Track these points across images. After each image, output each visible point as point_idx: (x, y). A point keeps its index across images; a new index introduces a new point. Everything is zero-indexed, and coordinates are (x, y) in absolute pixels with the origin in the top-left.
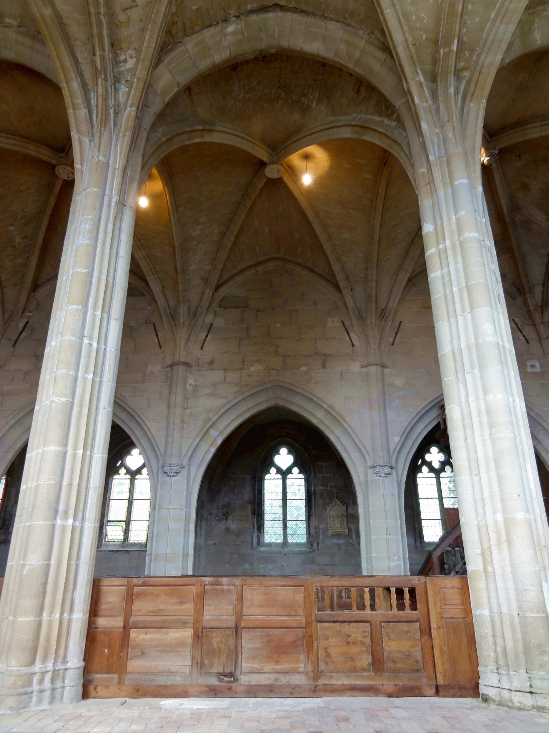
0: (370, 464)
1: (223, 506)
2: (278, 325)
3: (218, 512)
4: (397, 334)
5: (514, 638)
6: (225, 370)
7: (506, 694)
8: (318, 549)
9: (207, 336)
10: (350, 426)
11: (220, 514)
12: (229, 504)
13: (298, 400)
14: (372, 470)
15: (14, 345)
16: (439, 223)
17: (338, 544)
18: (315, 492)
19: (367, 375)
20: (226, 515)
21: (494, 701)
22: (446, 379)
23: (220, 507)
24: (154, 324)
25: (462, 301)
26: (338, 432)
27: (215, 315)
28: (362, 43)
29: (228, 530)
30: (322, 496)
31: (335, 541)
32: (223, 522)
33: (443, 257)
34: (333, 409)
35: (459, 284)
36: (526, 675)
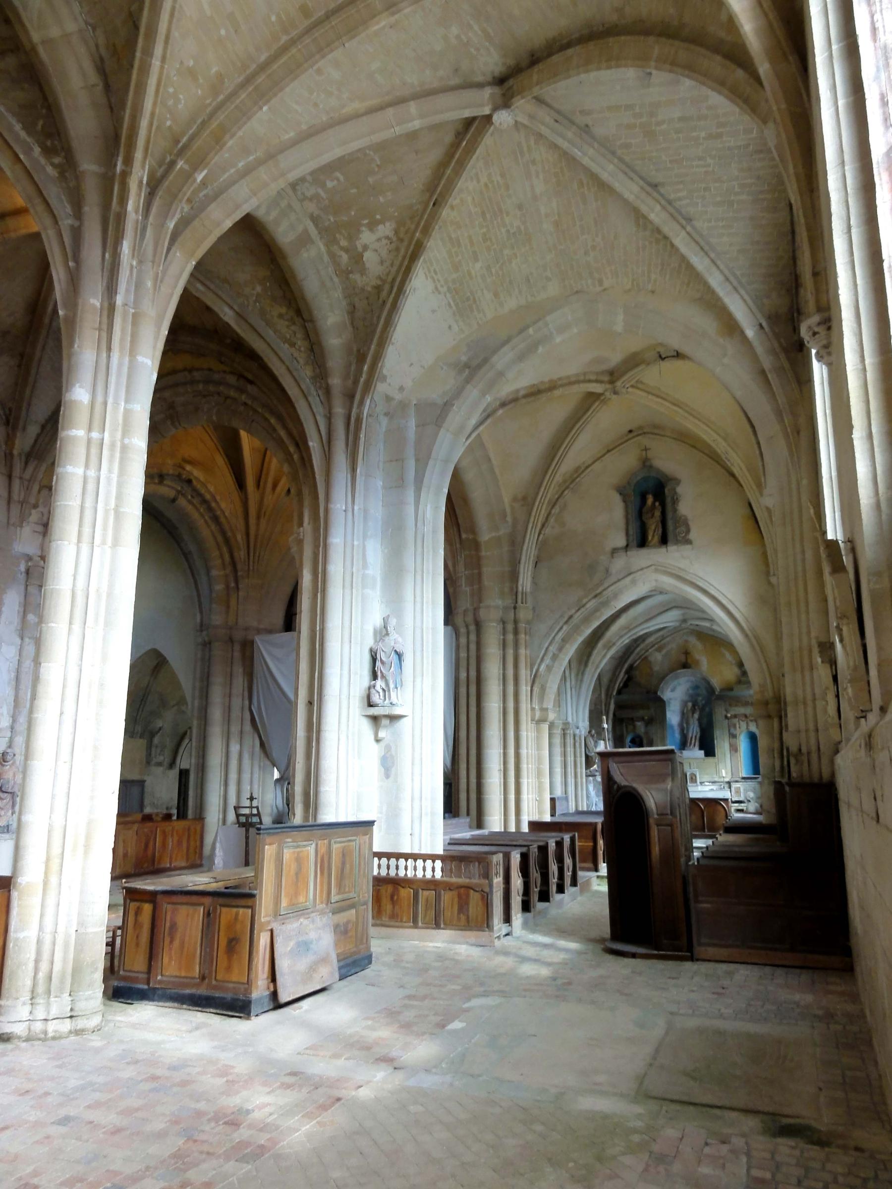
5: (65, 960)
7: (38, 1027)
16: (100, 399)
21: (19, 1038)
22: (53, 625)
25: (105, 528)
28: (71, 27)
33: (94, 451)
35: (107, 504)
36: (70, 999)
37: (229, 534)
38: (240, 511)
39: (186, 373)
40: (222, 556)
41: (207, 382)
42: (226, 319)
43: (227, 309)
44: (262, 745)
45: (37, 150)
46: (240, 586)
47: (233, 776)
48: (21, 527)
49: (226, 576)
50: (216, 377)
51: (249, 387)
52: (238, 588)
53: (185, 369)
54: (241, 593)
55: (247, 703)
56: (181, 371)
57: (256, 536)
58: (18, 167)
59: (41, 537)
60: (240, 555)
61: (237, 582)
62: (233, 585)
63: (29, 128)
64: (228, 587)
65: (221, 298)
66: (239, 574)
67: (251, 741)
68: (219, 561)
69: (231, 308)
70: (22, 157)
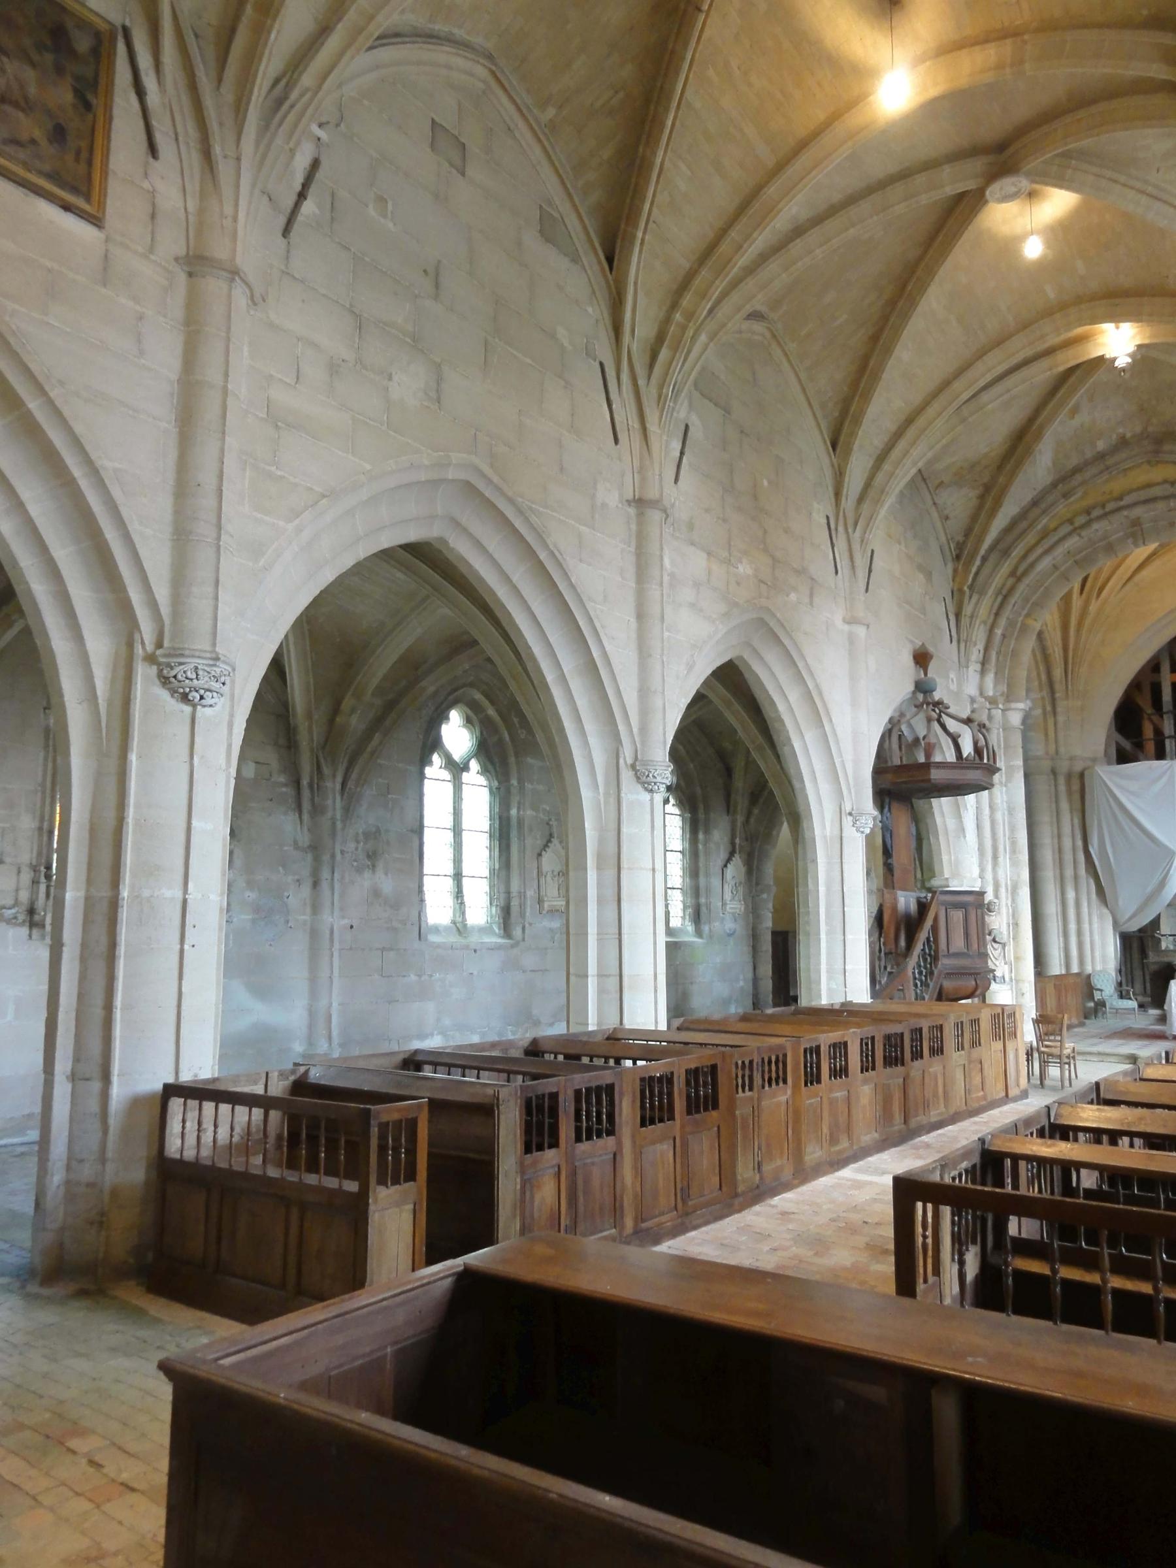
0: (848, 809)
1: (367, 835)
2: (766, 483)
3: (357, 849)
4: (870, 571)
6: (709, 554)
8: (524, 940)
9: (682, 453)
12: (378, 830)
13: (772, 657)
14: (850, 818)
15: (286, 231)
17: (551, 930)
23: (361, 837)
24: (601, 364)
26: (810, 736)
29: (376, 893)
30: (531, 830)
32: (367, 874)
34: (820, 694)
37: (1050, 651)
38: (1058, 624)
39: (1167, 486)
40: (1039, 675)
46: (1059, 709)
47: (1072, 927)
48: (967, 667)
49: (1043, 698)
52: (1055, 713)
53: (1165, 481)
54: (1061, 719)
55: (1080, 843)
56: (1158, 484)
59: (978, 676)
60: (1058, 673)
62: (1049, 708)
64: (1045, 713)
66: (1057, 695)
68: (1036, 683)
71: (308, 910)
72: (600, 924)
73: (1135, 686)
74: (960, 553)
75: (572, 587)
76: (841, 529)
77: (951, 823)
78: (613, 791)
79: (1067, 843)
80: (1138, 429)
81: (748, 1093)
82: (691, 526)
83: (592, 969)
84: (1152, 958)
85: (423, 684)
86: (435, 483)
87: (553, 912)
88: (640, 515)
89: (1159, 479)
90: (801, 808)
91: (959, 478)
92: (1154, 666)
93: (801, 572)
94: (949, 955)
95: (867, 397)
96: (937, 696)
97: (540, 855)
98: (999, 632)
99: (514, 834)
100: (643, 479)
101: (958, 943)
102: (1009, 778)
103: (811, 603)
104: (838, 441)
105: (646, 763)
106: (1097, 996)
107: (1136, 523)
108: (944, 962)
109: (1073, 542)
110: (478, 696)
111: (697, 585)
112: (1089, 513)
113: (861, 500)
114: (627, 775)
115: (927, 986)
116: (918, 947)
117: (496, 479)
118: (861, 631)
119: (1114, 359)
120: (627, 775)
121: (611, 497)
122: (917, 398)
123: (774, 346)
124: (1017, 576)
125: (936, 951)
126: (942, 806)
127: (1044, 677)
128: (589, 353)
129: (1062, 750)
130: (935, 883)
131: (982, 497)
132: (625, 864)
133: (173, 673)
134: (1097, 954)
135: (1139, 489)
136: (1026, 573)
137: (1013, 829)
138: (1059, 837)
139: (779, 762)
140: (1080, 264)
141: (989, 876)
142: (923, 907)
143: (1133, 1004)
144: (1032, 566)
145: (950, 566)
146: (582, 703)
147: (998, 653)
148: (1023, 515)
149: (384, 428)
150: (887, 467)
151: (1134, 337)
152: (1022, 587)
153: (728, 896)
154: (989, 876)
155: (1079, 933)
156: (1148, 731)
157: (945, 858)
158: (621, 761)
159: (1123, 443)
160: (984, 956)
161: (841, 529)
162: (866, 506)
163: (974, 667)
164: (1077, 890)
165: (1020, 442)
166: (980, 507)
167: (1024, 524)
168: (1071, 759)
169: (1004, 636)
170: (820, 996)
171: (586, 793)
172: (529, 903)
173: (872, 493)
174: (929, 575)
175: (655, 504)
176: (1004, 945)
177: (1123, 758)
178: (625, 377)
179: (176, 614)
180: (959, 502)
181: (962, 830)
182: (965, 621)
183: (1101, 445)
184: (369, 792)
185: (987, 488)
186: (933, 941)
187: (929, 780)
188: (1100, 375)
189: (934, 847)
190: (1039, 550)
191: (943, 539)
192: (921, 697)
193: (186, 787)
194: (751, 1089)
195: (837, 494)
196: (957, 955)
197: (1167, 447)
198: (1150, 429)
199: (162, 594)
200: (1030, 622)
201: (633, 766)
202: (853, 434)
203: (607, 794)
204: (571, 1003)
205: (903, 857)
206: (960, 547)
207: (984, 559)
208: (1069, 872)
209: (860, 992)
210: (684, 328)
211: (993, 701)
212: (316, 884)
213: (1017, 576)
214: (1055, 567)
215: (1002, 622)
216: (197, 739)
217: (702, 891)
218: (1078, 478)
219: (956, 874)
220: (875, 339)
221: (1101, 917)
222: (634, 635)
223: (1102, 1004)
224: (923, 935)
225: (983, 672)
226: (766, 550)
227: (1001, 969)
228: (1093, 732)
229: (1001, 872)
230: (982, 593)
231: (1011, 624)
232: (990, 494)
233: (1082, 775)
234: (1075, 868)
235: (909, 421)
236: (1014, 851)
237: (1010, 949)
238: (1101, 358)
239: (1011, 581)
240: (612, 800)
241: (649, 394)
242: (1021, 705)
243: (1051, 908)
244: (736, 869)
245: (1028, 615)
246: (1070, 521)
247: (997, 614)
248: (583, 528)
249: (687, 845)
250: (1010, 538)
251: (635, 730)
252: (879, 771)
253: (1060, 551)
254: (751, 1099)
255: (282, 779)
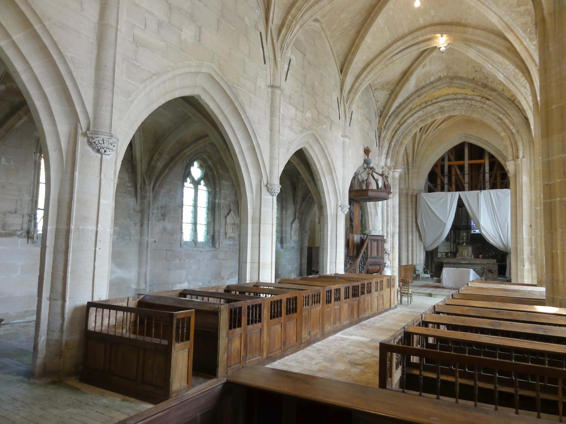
1: (162, 207)
6: (296, 109)
10: (337, 177)
11: (159, 215)
12: (166, 206)
17: (229, 245)
18: (219, 205)
19: (344, 143)
20: (164, 215)
23: (160, 208)
26: (328, 178)
27: (292, 53)
29: (165, 229)
30: (223, 208)
31: (228, 242)
32: (162, 222)
34: (332, 163)
41: (465, 99)
42: (500, 79)
43: (500, 75)
44: (420, 236)
45: (528, 40)
47: (410, 248)
50: (469, 97)
51: (488, 102)
52: (408, 173)
53: (453, 93)
54: (410, 176)
55: (414, 220)
57: (417, 152)
58: (522, 46)
59: (385, 159)
61: (408, 171)
63: (524, 31)
65: (499, 71)
66: (410, 167)
67: (416, 234)
69: (502, 74)
70: (524, 43)
71: (139, 235)
72: (252, 244)
73: (436, 165)
74: (382, 115)
75: (247, 117)
76: (342, 102)
77: (373, 211)
78: (259, 195)
79: (410, 219)
80: (446, 74)
81: (307, 307)
82: (290, 98)
83: (249, 260)
84: (436, 260)
85: (185, 151)
86: (198, 73)
87: (230, 238)
88: (273, 92)
89: (451, 92)
90: (323, 204)
91: (382, 88)
92: (442, 159)
93: (328, 117)
94: (371, 257)
95: (354, 54)
96: (371, 165)
97: (226, 217)
98: (393, 144)
99: (217, 209)
100: (274, 78)
101: (375, 254)
102: (393, 196)
103: (331, 129)
104: (343, 70)
105: (271, 185)
106: (417, 272)
107: (442, 107)
108: (369, 260)
109: (420, 113)
110: (205, 157)
111: (291, 119)
112: (426, 103)
113: (350, 92)
114: (264, 189)
115: (363, 268)
116: (361, 255)
117: (220, 73)
118: (347, 140)
119: (440, 48)
120: (264, 189)
121: (262, 84)
122: (372, 56)
123: (322, 32)
124: (400, 124)
125: (367, 256)
126: (370, 205)
127: (406, 160)
128: (256, 28)
129: (410, 187)
130: (366, 232)
131: (390, 95)
132: (262, 222)
133: (94, 141)
134: (418, 258)
135: (444, 95)
136: (403, 123)
137: (394, 214)
138: (407, 217)
139: (316, 187)
140: (432, 11)
141: (385, 230)
142: (363, 241)
143: (429, 276)
144: (406, 121)
145: (378, 119)
146: (249, 161)
147: (392, 151)
148: (404, 102)
149: (179, 50)
150: (359, 81)
151: (447, 40)
152: (402, 128)
153: (293, 234)
154: (385, 230)
155: (412, 251)
156: (439, 182)
157: (370, 223)
158: (262, 184)
159: (440, 79)
160: (383, 258)
161: (342, 102)
162: (351, 94)
163: (384, 156)
164: (412, 236)
165: (405, 75)
166: (389, 99)
167: (404, 105)
168: (413, 190)
169: (395, 145)
170: (327, 271)
171: (249, 195)
172: (221, 234)
173: (353, 90)
174: (370, 122)
175: (279, 88)
176: (389, 254)
177: (430, 190)
178: (269, 38)
179: (95, 118)
180: (382, 96)
181: (377, 214)
182: (382, 139)
183: (432, 79)
184: (163, 191)
185: (392, 92)
186: (366, 253)
187: (367, 195)
188: (434, 53)
189: (367, 219)
190: (409, 115)
191: (376, 109)
192: (366, 166)
193: (98, 186)
194: (308, 305)
195: (341, 90)
196: (374, 258)
197: (455, 81)
198: (449, 74)
199: (90, 109)
200: (404, 141)
201: (267, 186)
202: (348, 68)
203: (256, 195)
204: (241, 272)
205: (356, 222)
206: (382, 112)
207: (390, 117)
208: (410, 230)
209: (341, 270)
210: (292, 22)
211: (390, 168)
212: (142, 225)
213: (400, 124)
214: (414, 122)
215: (394, 140)
216: (103, 167)
217: (284, 232)
218: (424, 90)
219: (374, 229)
220: (358, 32)
221: (420, 245)
222: (269, 137)
223: (419, 275)
224: (363, 250)
225: (387, 158)
226: (316, 108)
227: (388, 263)
228: (422, 180)
229: (389, 229)
230: (388, 129)
231: (397, 141)
232: (393, 94)
233: (416, 196)
234: (412, 228)
235: (368, 64)
236: (394, 222)
237: (391, 255)
238: (436, 47)
239: (398, 125)
240: (258, 198)
241: (278, 46)
242: (399, 170)
243: (404, 242)
244: (296, 225)
245: (403, 138)
246: (420, 105)
247: (393, 137)
248: (251, 95)
249: (279, 215)
250: (399, 110)
251: (268, 173)
252: (351, 191)
253: (416, 116)
254: (308, 309)
255: (130, 185)
